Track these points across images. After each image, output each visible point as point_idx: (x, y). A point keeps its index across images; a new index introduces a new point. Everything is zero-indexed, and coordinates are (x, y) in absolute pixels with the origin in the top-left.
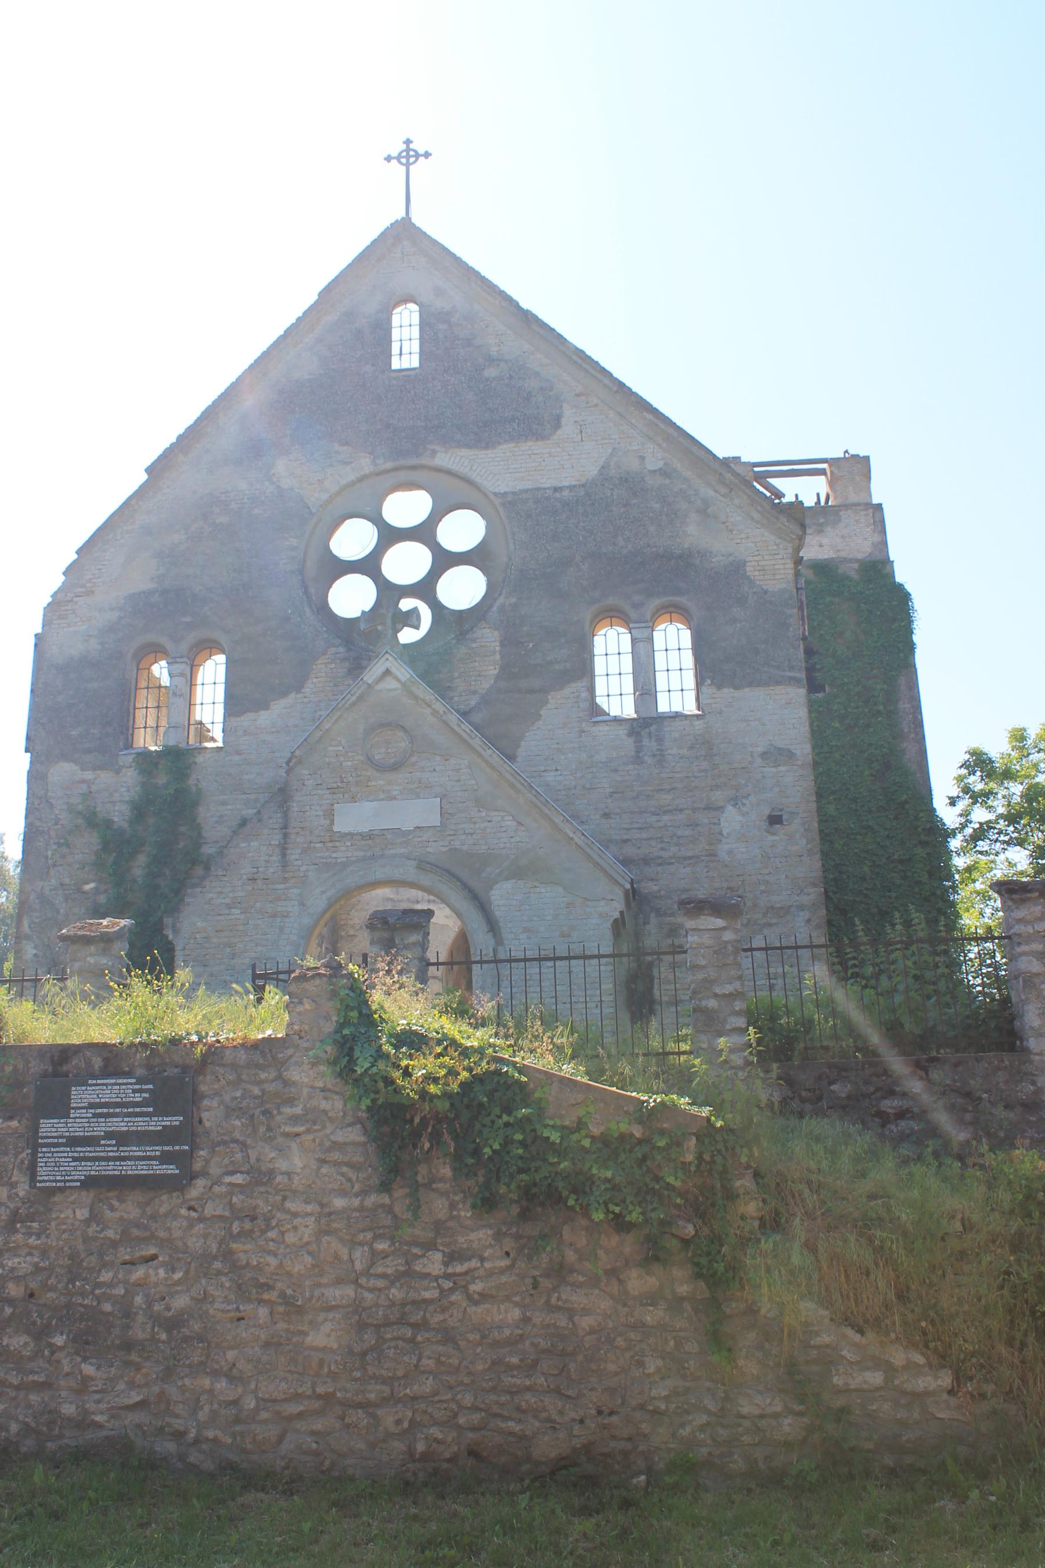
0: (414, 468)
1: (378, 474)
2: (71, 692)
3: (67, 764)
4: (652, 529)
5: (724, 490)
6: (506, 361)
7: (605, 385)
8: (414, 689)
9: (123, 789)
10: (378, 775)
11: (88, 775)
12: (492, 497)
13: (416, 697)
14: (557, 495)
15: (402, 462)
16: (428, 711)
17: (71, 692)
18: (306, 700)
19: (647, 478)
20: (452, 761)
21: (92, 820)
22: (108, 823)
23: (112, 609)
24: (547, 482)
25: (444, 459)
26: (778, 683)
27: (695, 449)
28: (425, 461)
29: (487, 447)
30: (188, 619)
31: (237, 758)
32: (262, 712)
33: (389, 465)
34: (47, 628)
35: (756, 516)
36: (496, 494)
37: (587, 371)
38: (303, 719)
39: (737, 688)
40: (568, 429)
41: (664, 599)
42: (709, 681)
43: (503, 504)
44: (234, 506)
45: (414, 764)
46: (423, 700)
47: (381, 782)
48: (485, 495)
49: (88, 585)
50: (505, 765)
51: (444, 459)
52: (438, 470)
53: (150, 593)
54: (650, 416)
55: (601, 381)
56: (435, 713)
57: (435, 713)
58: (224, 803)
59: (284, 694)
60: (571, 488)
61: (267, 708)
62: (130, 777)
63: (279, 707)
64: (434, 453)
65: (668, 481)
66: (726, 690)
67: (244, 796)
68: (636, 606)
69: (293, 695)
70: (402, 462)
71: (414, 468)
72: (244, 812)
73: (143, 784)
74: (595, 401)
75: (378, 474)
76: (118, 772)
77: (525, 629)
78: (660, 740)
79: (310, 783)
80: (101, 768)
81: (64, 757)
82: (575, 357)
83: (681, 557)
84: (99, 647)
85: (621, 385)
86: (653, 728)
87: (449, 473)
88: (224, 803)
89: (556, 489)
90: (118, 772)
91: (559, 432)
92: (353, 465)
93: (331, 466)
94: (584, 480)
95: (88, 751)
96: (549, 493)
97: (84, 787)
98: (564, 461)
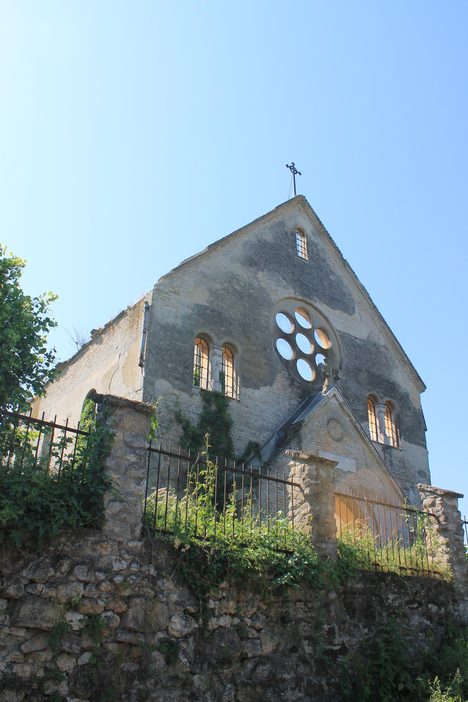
0: (307, 303)
1: (295, 299)
2: (168, 342)
3: (165, 381)
4: (384, 368)
5: (402, 363)
6: (337, 276)
7: (369, 304)
8: (344, 407)
9: (194, 406)
10: (333, 441)
11: (176, 392)
12: (335, 330)
13: (344, 410)
14: (356, 340)
15: (305, 299)
16: (348, 419)
17: (168, 342)
18: (274, 391)
19: (381, 348)
20: (357, 445)
21: (179, 418)
22: (188, 422)
23: (188, 307)
24: (353, 333)
25: (319, 305)
26: (421, 445)
27: (396, 343)
28: (313, 303)
29: (333, 308)
30: (224, 329)
31: (246, 409)
32: (256, 390)
33: (300, 297)
34: (155, 302)
35: (411, 377)
36: (337, 330)
37: (364, 295)
38: (273, 400)
39: (410, 443)
40: (356, 315)
41: (389, 399)
42: (403, 437)
43: (339, 336)
44: (241, 283)
45: (345, 441)
46: (347, 413)
47: (335, 446)
48: (332, 328)
49: (176, 289)
50: (376, 453)
51: (319, 305)
52: (316, 308)
53: (206, 308)
54: (383, 324)
55: (368, 302)
56: (351, 421)
57: (351, 421)
58: (241, 430)
59: (266, 385)
60: (360, 340)
61: (259, 389)
62: (198, 400)
63: (264, 390)
64: (316, 301)
65: (386, 352)
66: (407, 442)
67: (250, 430)
68: (382, 398)
69: (268, 387)
70: (305, 299)
71: (307, 303)
72: (250, 438)
73: (204, 408)
74: (364, 308)
75: (295, 299)
76: (191, 396)
77: (349, 392)
78: (391, 456)
79: (308, 436)
80: (183, 390)
81: (164, 376)
82: (360, 288)
83: (392, 383)
84: (182, 324)
85: (375, 307)
86: (389, 450)
87: (320, 312)
88: (241, 430)
89: (355, 338)
90: (191, 396)
91: (354, 314)
92: (288, 290)
93: (279, 286)
94: (363, 339)
95: (177, 379)
96: (353, 338)
97: (174, 397)
98: (358, 327)
